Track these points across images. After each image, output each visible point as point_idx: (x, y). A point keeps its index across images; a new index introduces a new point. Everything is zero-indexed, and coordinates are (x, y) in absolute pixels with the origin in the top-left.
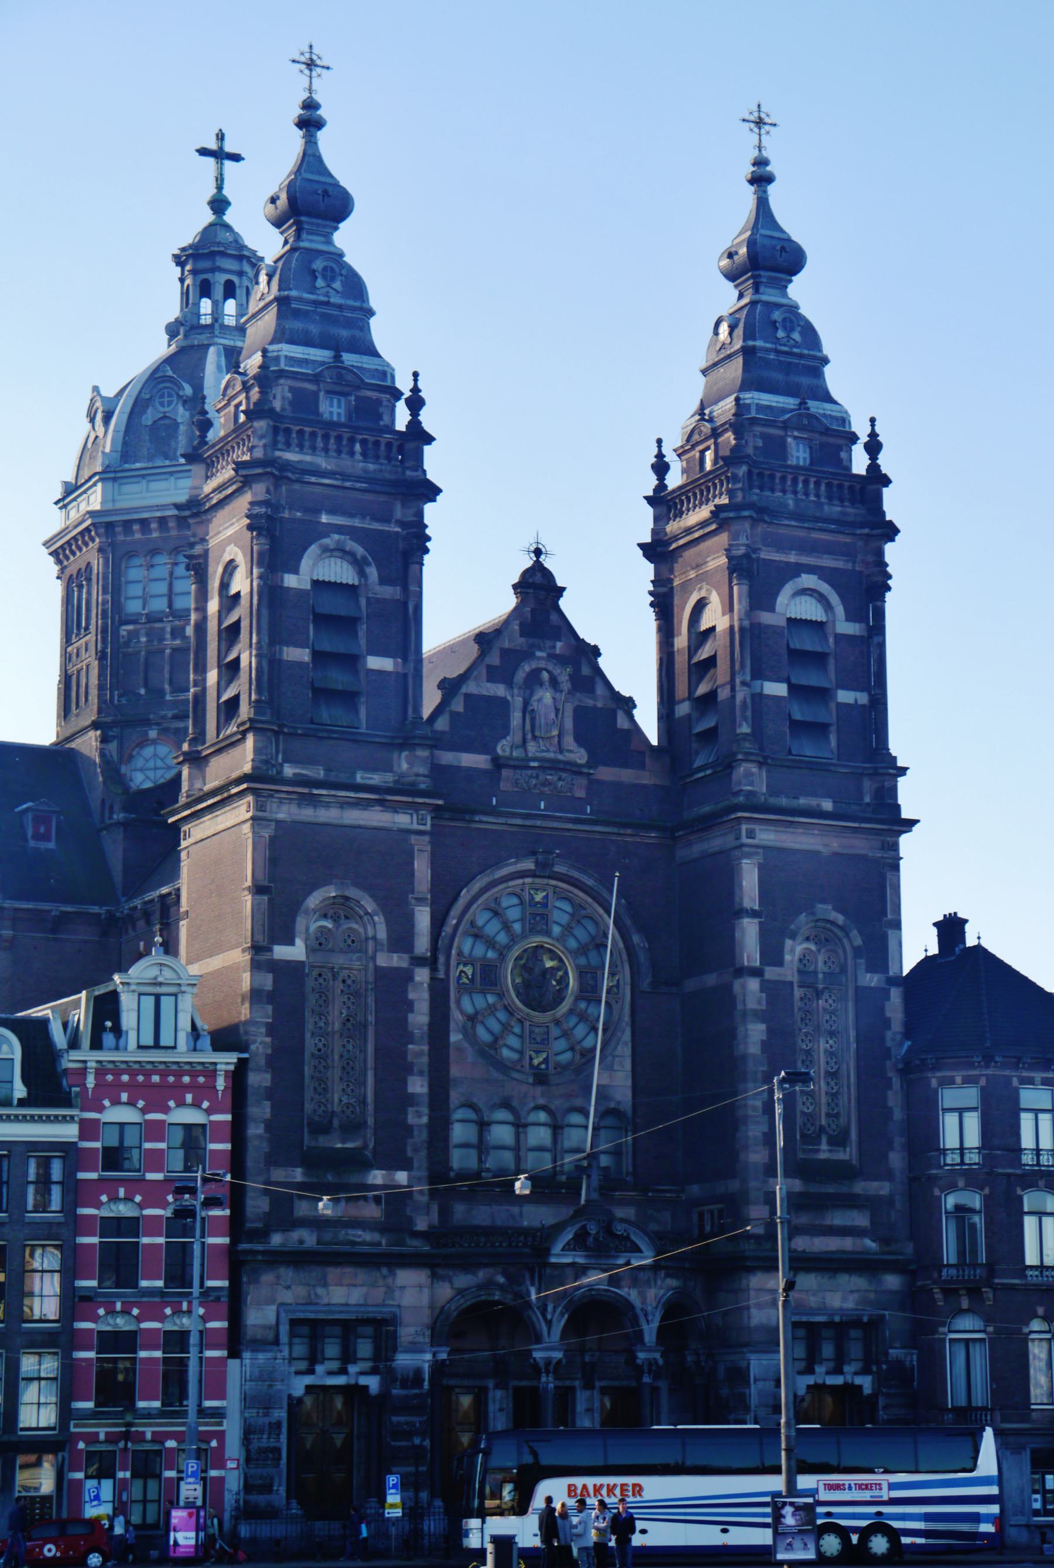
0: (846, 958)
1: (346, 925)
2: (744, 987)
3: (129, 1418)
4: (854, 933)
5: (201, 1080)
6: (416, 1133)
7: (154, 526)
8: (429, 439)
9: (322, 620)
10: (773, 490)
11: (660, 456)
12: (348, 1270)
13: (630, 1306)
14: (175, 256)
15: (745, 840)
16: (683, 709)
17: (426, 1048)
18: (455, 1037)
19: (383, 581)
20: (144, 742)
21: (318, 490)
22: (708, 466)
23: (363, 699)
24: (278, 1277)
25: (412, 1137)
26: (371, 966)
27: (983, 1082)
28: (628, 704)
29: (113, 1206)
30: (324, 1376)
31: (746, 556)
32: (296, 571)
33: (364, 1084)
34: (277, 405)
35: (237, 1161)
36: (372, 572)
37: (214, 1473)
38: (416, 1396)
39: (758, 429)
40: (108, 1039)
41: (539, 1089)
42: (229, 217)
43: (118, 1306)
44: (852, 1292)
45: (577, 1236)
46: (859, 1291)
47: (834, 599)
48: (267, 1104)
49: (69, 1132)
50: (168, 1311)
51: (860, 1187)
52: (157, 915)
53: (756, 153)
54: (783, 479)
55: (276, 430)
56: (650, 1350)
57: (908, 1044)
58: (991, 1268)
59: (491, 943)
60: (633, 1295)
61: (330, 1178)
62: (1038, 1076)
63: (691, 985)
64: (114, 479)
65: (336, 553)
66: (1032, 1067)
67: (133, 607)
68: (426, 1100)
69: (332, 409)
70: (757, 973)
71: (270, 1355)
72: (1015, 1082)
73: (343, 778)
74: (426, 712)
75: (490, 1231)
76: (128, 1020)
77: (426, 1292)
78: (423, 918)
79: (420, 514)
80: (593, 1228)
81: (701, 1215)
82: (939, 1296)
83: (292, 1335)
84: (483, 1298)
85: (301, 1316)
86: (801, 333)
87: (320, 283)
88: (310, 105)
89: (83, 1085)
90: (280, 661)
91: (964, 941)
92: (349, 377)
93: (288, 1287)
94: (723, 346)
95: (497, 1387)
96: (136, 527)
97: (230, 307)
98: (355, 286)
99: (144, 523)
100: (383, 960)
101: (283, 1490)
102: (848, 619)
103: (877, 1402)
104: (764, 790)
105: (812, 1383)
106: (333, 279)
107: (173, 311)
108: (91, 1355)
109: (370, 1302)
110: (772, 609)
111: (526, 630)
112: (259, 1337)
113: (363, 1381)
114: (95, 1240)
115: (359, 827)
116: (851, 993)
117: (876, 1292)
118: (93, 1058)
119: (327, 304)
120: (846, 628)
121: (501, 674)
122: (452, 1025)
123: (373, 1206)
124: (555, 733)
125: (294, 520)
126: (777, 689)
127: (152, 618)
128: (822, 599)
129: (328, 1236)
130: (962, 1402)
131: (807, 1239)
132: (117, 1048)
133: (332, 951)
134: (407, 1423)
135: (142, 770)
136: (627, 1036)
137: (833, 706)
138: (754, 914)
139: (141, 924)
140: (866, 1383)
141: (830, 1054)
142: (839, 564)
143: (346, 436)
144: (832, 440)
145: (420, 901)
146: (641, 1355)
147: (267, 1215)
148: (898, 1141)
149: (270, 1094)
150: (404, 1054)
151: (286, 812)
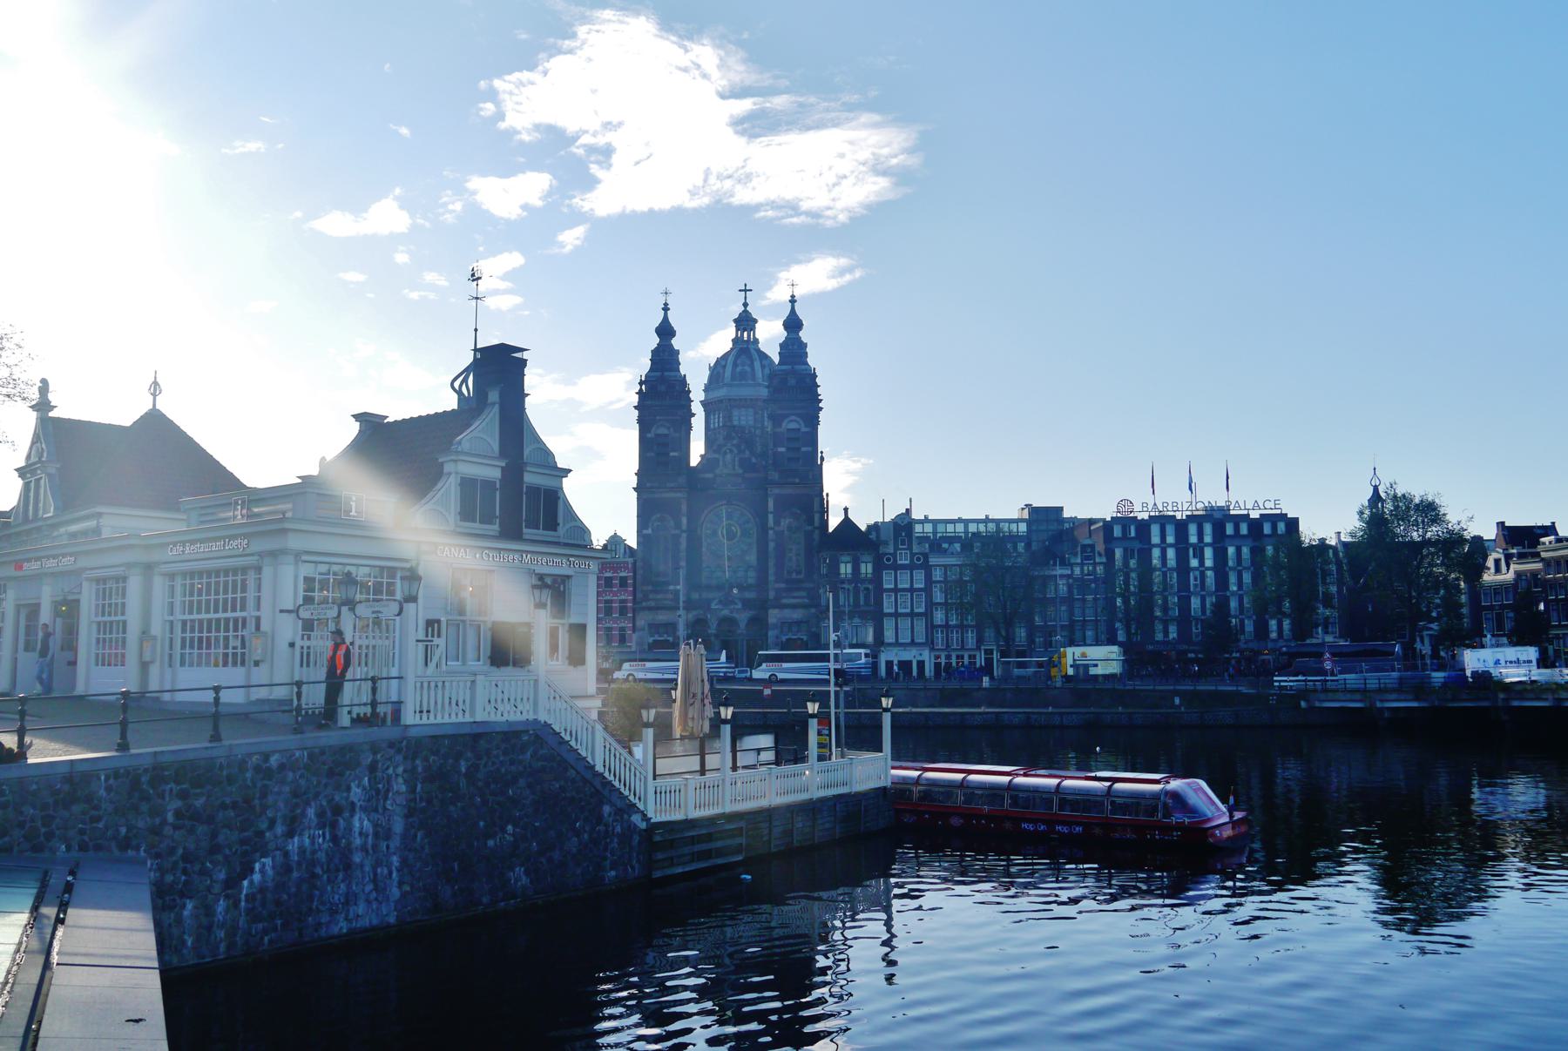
30: (657, 638)
32: (650, 432)
36: (672, 430)
47: (801, 422)
60: (735, 615)
69: (663, 388)
78: (684, 520)
88: (666, 304)
100: (674, 532)
102: (806, 426)
107: (734, 336)
110: (780, 426)
120: (804, 429)
127: (715, 429)
128: (798, 422)
138: (771, 513)
140: (805, 638)
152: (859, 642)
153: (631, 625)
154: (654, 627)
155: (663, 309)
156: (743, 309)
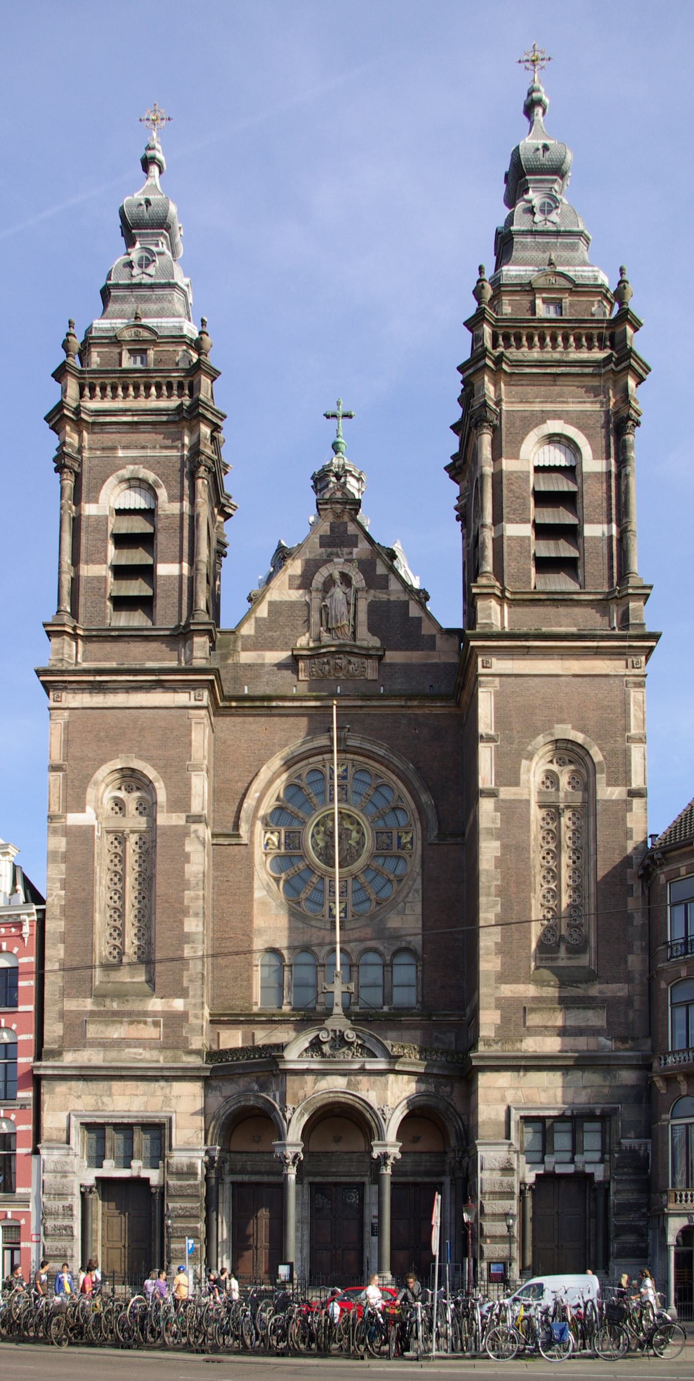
0: (588, 776)
5: (13, 930)
9: (122, 541)
24: (70, 1089)
25: (188, 970)
32: (96, 501)
44: (584, 1087)
46: (592, 1086)
48: (61, 946)
51: (595, 990)
61: (115, 1006)
65: (133, 483)
82: (660, 1084)
84: (242, 1103)
93: (79, 1097)
103: (609, 1188)
105: (541, 1172)
109: (149, 1109)
112: (55, 1138)
113: (145, 1173)
117: (610, 1087)
123: (152, 1029)
134: (181, 1209)
147: (63, 1037)
148: (638, 944)
150: (181, 900)
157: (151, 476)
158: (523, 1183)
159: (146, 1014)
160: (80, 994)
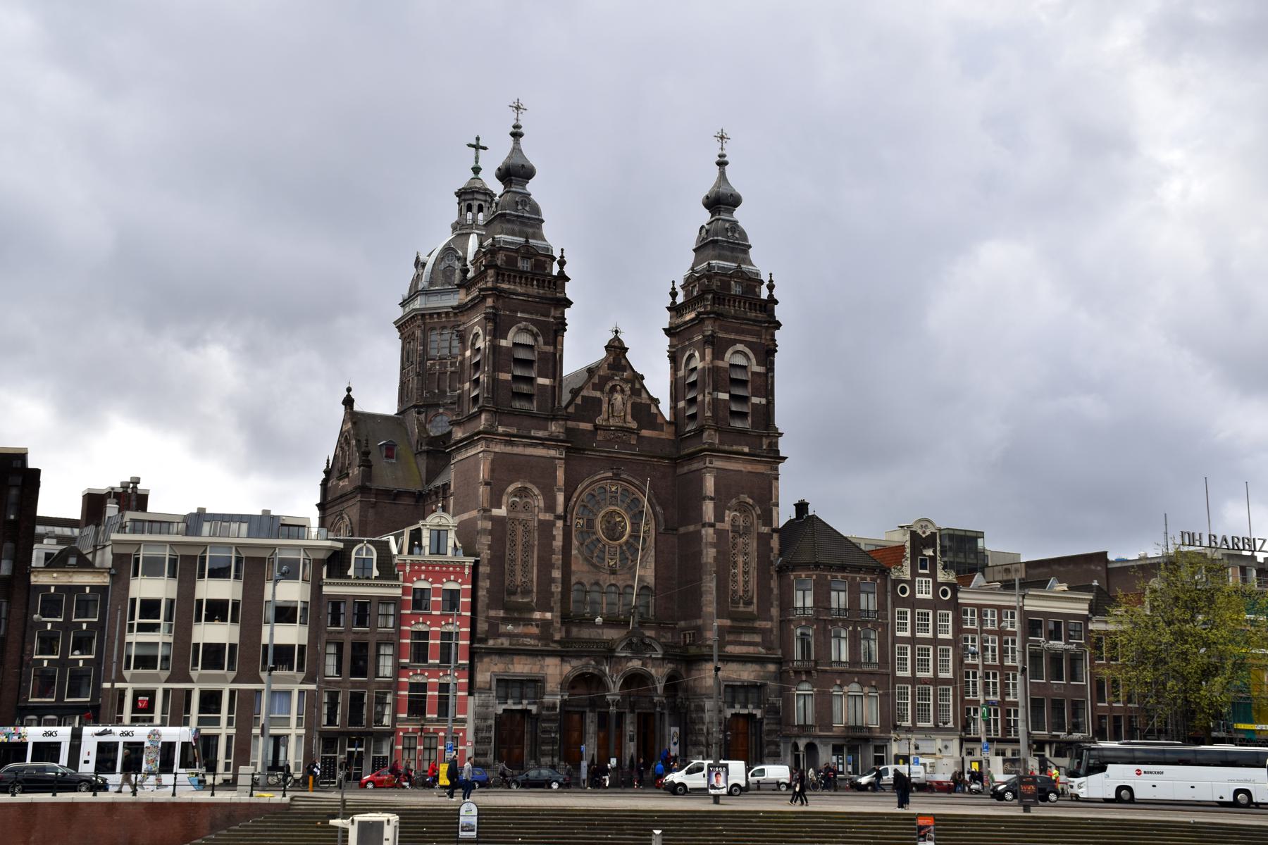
1: (525, 500)
2: (706, 531)
3: (422, 722)
4: (757, 508)
5: (458, 569)
6: (555, 595)
7: (443, 315)
8: (568, 279)
10: (724, 305)
11: (674, 289)
12: (524, 657)
13: (651, 676)
14: (456, 193)
15: (708, 464)
16: (681, 404)
17: (561, 557)
18: (574, 552)
19: (546, 343)
20: (438, 414)
21: (516, 301)
22: (695, 293)
23: (535, 397)
26: (536, 519)
27: (814, 577)
28: (656, 402)
29: (417, 626)
30: (510, 705)
31: (712, 335)
32: (506, 338)
33: (532, 573)
34: (499, 263)
35: (473, 607)
36: (541, 339)
37: (461, 748)
38: (553, 715)
39: (718, 277)
40: (416, 550)
41: (612, 576)
42: (480, 176)
43: (419, 671)
45: (627, 644)
47: (751, 355)
49: (398, 592)
50: (441, 674)
51: (758, 624)
52: (441, 493)
53: (720, 152)
54: (729, 301)
55: (497, 274)
56: (659, 696)
57: (781, 559)
58: (816, 662)
59: (591, 511)
60: (653, 671)
61: (516, 615)
62: (839, 575)
63: (682, 530)
64: (426, 294)
66: (836, 571)
67: (433, 353)
68: (560, 580)
69: (524, 265)
70: (712, 525)
71: (487, 695)
72: (829, 577)
73: (525, 433)
74: (564, 404)
75: (589, 641)
76: (426, 541)
77: (559, 668)
78: (560, 498)
79: (563, 313)
80: (635, 640)
81: (685, 635)
83: (498, 686)
85: (501, 677)
86: (739, 234)
87: (520, 207)
89: (404, 571)
90: (498, 380)
91: (807, 513)
92: (532, 251)
93: (496, 664)
94: (703, 239)
95: (591, 711)
96: (435, 316)
97: (481, 215)
98: (536, 209)
99: (439, 314)
100: (542, 516)
101: (492, 756)
102: (757, 365)
104: (717, 442)
106: (526, 205)
108: (406, 693)
110: (723, 359)
111: (610, 367)
113: (529, 707)
114: (409, 641)
115: (532, 456)
116: (756, 535)
118: (409, 558)
119: (523, 217)
121: (599, 387)
122: (573, 546)
124: (622, 414)
125: (506, 315)
126: (725, 396)
128: (746, 355)
129: (514, 642)
130: (802, 723)
131: (732, 646)
132: (420, 554)
133: (519, 512)
135: (436, 427)
136: (653, 553)
137: (750, 404)
138: (711, 499)
139: (434, 497)
140: (758, 713)
141: (745, 563)
142: (755, 340)
143: (530, 277)
144: (752, 283)
145: (559, 490)
146: (656, 699)
147: (487, 631)
148: (775, 603)
149: (489, 576)
150: (550, 559)
151: (499, 448)
152: (859, 724)
153: (465, 681)
154: (506, 685)
155: (513, 135)
156: (472, 175)
157: (535, 330)
158: (726, 718)
159: (532, 620)
160: (496, 608)
